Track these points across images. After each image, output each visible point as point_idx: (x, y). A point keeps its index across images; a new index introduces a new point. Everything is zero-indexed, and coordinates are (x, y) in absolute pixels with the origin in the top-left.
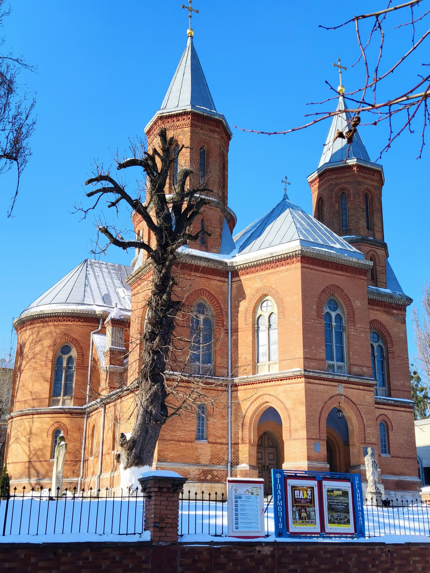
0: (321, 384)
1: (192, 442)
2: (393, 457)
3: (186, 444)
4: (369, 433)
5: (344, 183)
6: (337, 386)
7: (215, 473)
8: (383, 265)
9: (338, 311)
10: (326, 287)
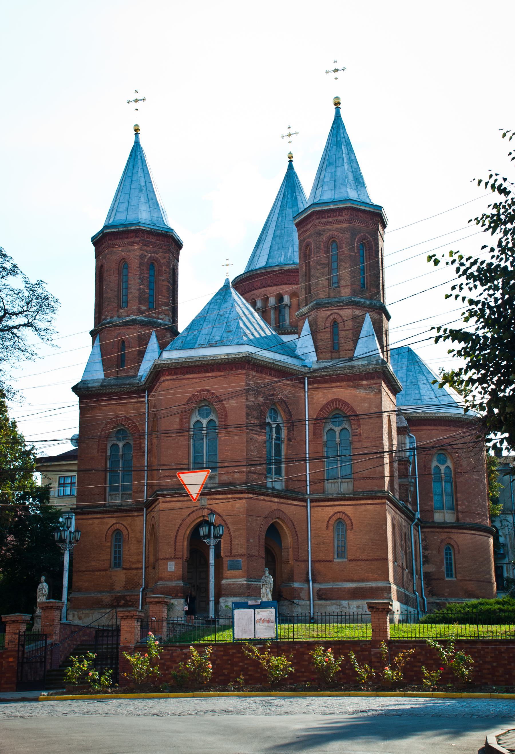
0: (179, 501)
1: (105, 570)
2: (350, 561)
4: (237, 544)
7: (128, 598)
8: (348, 328)
9: (212, 417)
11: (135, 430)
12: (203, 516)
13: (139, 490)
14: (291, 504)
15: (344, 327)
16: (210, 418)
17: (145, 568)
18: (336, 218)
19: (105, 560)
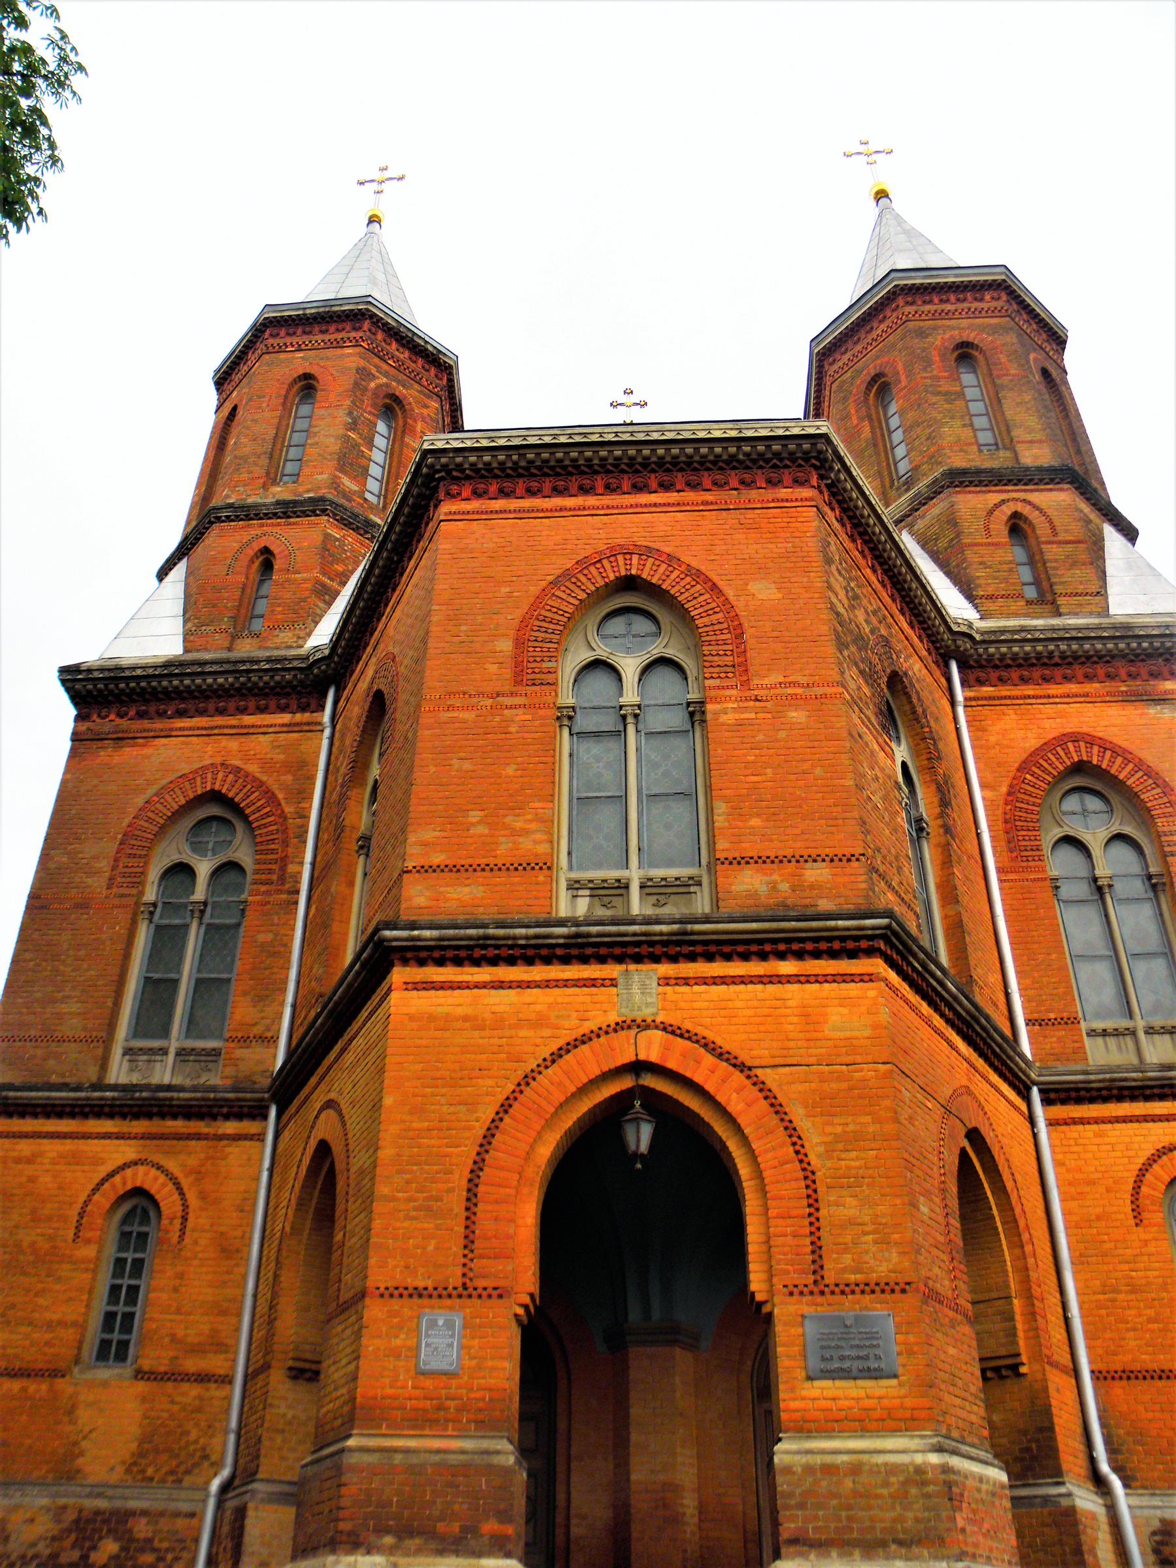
0: (500, 985)
3: (24, 1389)
4: (852, 1222)
5: (877, 357)
6: (613, 983)
10: (577, 563)
11: (267, 815)
12: (638, 1067)
13: (257, 1030)
14: (992, 1085)
15: (1055, 534)
16: (657, 649)
17: (246, 1376)
18: (965, 305)
19: (62, 1323)
